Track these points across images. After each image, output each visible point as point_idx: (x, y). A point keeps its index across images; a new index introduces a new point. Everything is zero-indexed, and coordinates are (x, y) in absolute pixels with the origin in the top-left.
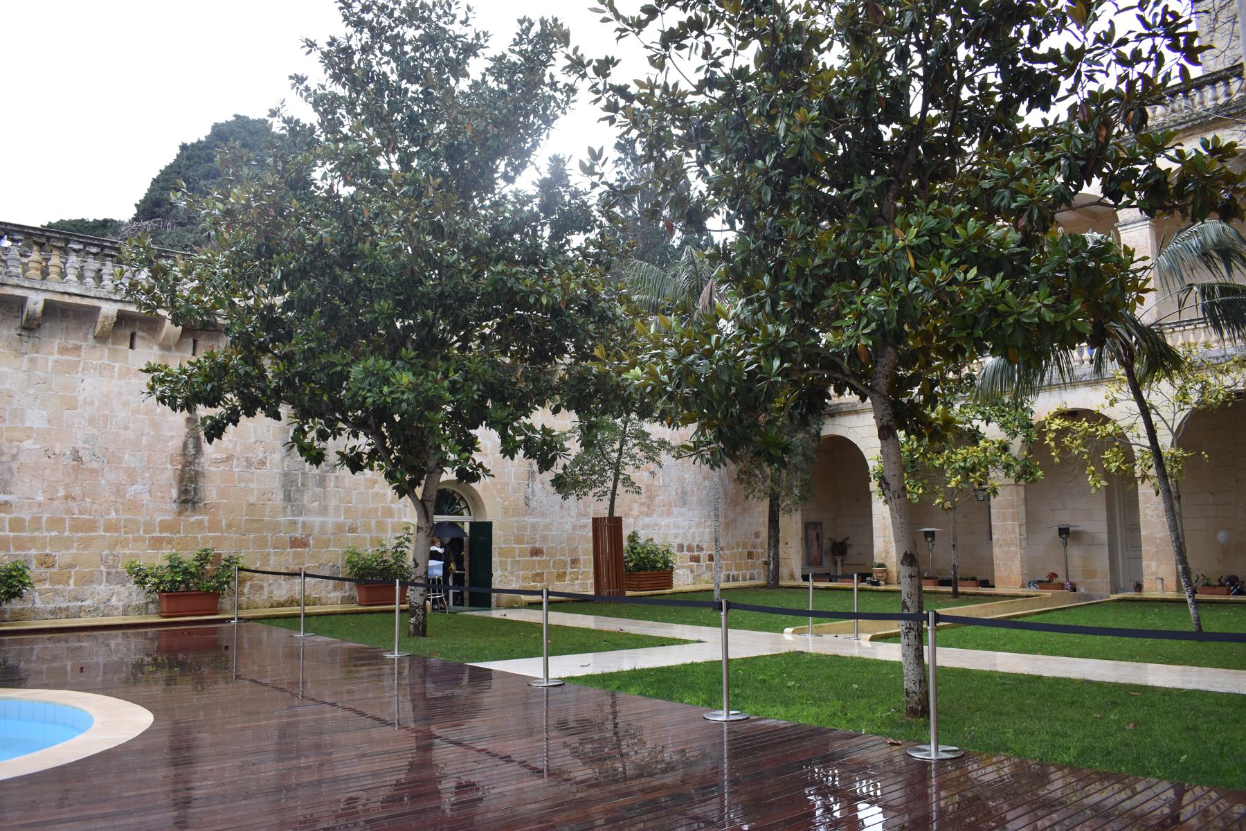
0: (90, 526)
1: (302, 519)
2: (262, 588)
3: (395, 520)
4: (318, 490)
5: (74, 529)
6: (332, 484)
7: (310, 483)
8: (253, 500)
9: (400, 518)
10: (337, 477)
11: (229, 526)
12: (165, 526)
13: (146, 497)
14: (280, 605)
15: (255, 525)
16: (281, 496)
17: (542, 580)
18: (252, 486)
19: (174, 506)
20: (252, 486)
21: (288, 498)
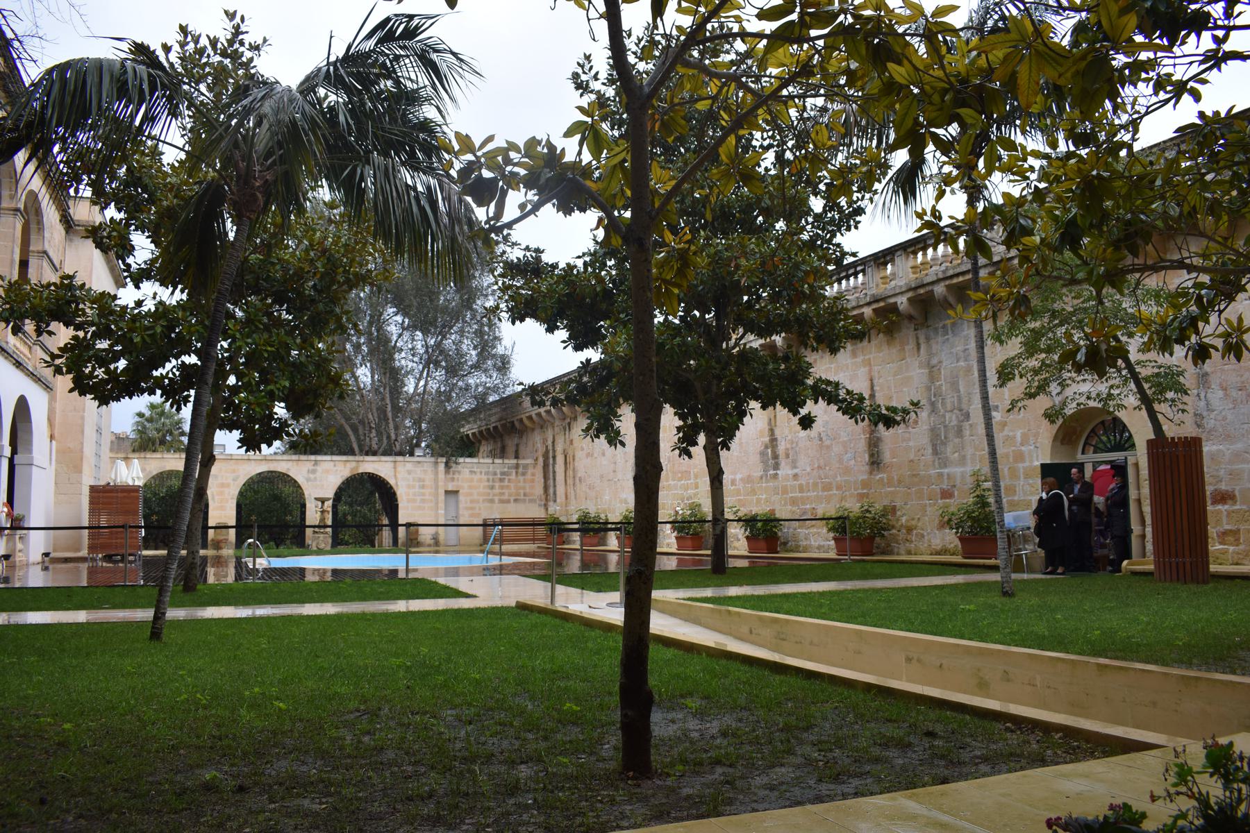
0: (827, 487)
1: (946, 471)
2: (923, 536)
3: (1027, 464)
4: (957, 440)
5: (824, 489)
6: (968, 433)
7: (951, 435)
8: (912, 457)
9: (1031, 461)
10: (971, 426)
11: (900, 482)
12: (865, 484)
13: (852, 462)
14: (938, 553)
15: (916, 480)
16: (930, 451)
17: (1237, 542)
18: (911, 444)
19: (867, 468)
20: (911, 444)
21: (935, 452)
